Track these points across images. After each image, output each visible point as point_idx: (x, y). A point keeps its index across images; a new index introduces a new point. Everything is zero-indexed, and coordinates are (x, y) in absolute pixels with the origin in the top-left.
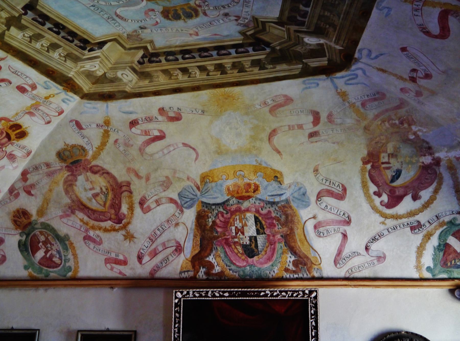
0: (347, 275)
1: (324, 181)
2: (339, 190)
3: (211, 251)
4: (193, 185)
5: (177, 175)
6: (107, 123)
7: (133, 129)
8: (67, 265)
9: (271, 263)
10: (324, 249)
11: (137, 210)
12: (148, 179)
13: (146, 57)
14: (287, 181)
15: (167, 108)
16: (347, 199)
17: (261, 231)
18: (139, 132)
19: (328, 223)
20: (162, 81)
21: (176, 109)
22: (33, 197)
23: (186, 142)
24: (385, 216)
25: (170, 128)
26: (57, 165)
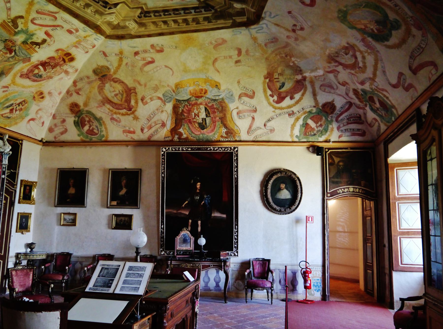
0: (254, 140)
1: (243, 88)
2: (251, 93)
3: (181, 126)
4: (170, 89)
5: (162, 84)
6: (121, 53)
7: (137, 57)
8: (102, 134)
9: (213, 133)
10: (242, 126)
11: (140, 103)
12: (145, 86)
13: (143, 13)
14: (223, 88)
15: (155, 45)
16: (255, 98)
17: (208, 115)
18: (139, 59)
19: (245, 111)
20: (152, 28)
21: (160, 46)
22: (81, 96)
23: (167, 65)
24: (275, 108)
25: (157, 57)
26: (93, 77)
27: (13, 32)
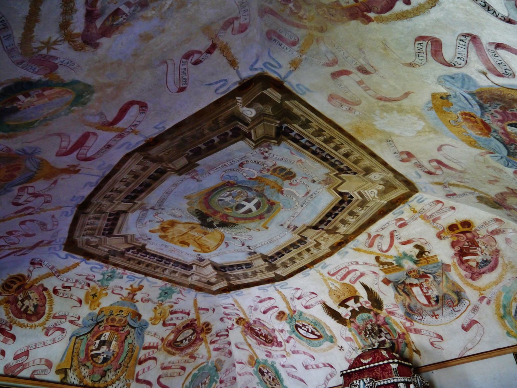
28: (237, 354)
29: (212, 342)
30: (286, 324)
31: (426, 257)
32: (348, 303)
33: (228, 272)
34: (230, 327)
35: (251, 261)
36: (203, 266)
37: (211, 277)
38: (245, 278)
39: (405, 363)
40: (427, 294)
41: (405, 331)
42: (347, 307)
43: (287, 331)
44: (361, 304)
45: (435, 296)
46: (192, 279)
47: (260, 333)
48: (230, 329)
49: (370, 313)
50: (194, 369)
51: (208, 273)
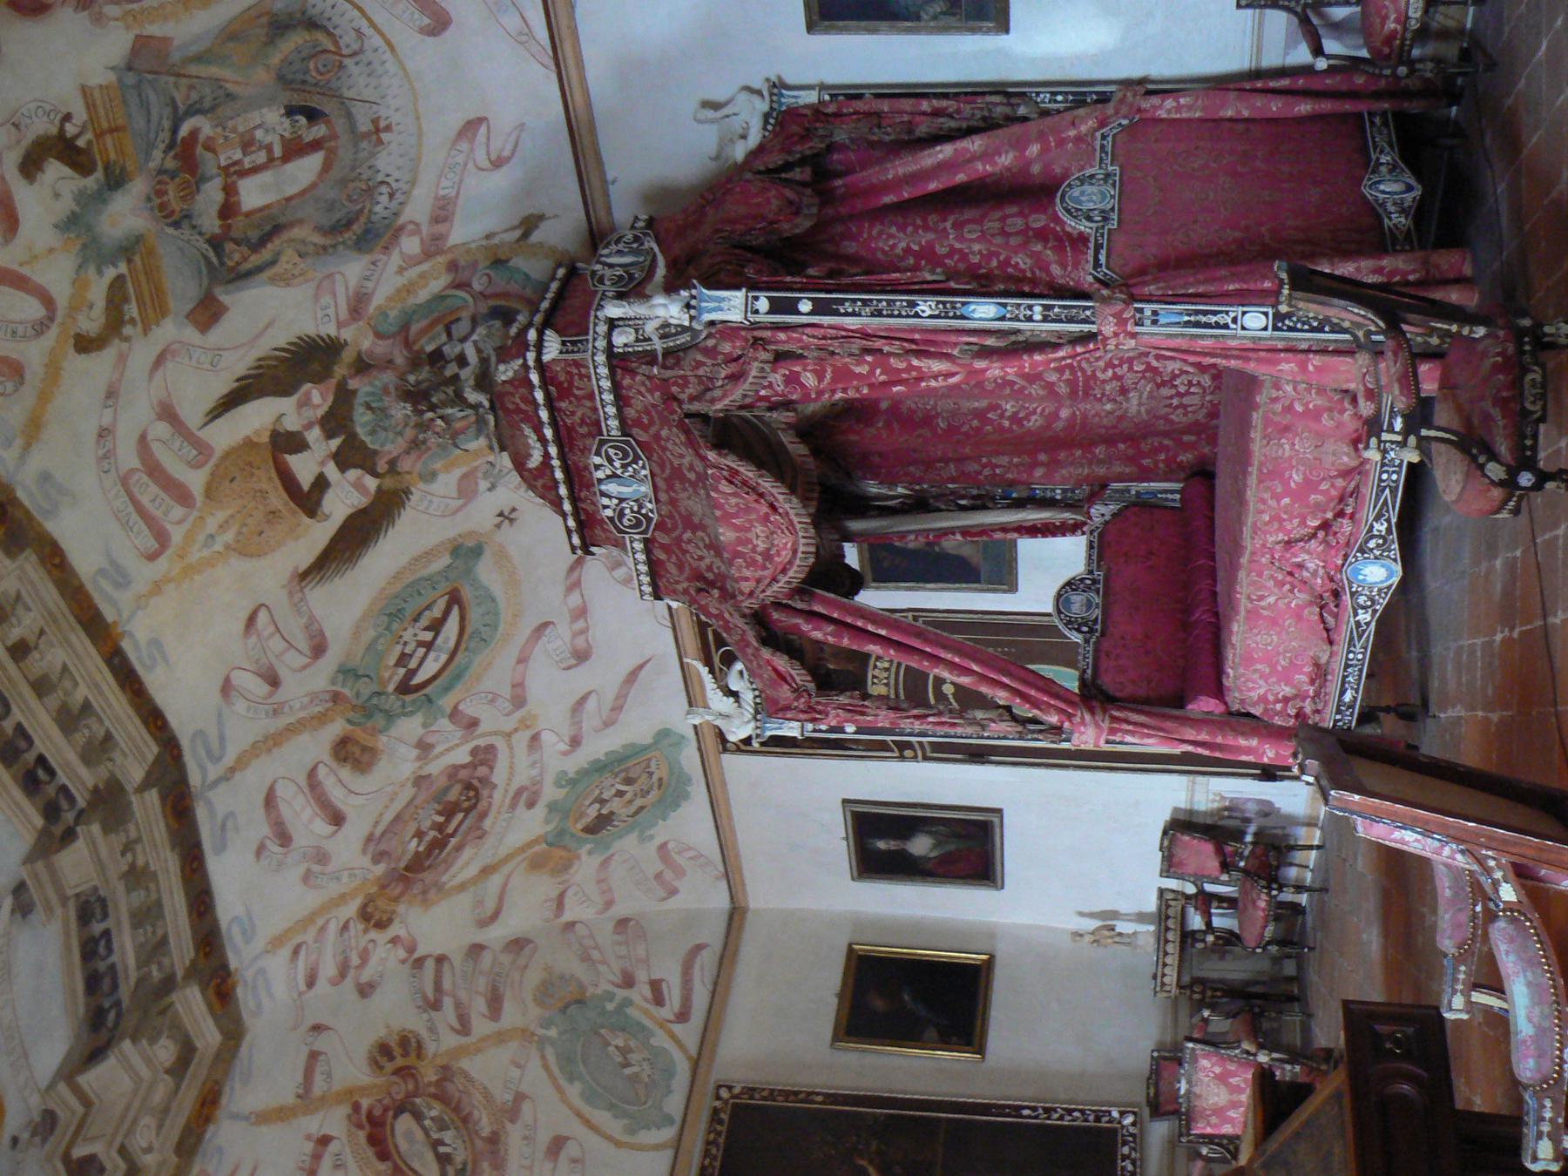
27: (137, 259)
28: (526, 909)
29: (464, 1027)
30: (393, 732)
31: (89, 136)
32: (305, 479)
33: (125, 992)
34: (402, 954)
35: (64, 901)
36: (80, 1110)
37: (148, 1061)
38: (161, 916)
39: (550, 295)
40: (278, 151)
41: (441, 260)
42: (321, 483)
43: (424, 725)
44: (309, 426)
45: (287, 122)
46: (149, 1150)
47: (433, 833)
48: (411, 949)
49: (354, 393)
50: (564, 1099)
51: (127, 1084)
